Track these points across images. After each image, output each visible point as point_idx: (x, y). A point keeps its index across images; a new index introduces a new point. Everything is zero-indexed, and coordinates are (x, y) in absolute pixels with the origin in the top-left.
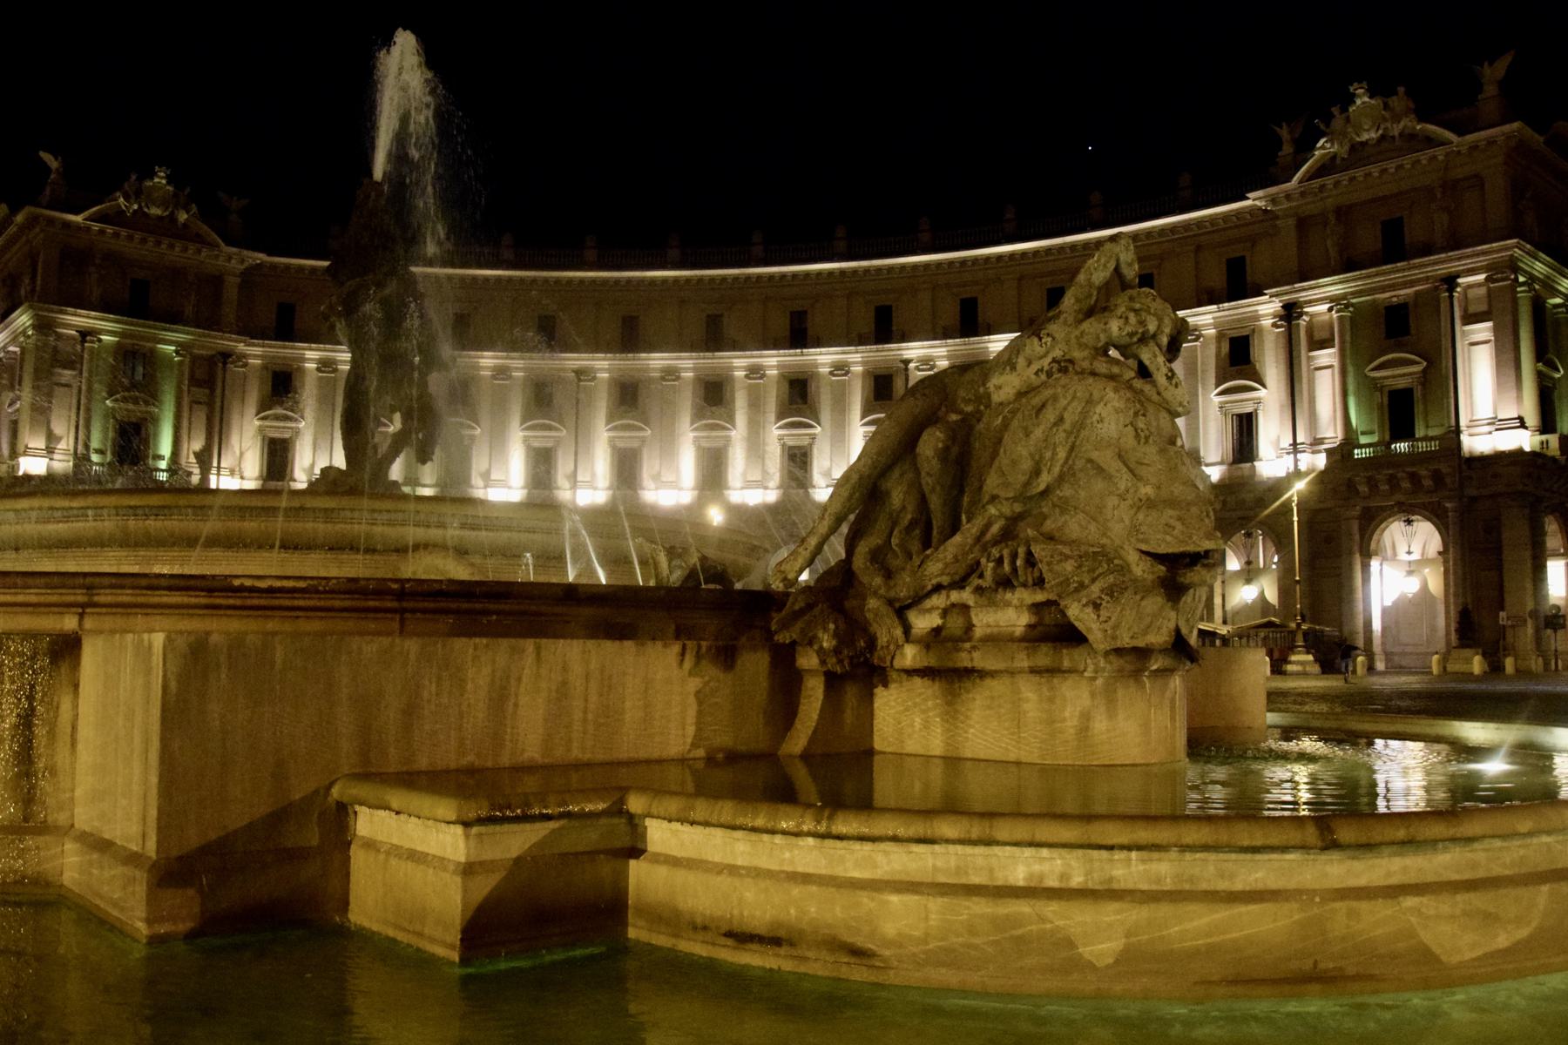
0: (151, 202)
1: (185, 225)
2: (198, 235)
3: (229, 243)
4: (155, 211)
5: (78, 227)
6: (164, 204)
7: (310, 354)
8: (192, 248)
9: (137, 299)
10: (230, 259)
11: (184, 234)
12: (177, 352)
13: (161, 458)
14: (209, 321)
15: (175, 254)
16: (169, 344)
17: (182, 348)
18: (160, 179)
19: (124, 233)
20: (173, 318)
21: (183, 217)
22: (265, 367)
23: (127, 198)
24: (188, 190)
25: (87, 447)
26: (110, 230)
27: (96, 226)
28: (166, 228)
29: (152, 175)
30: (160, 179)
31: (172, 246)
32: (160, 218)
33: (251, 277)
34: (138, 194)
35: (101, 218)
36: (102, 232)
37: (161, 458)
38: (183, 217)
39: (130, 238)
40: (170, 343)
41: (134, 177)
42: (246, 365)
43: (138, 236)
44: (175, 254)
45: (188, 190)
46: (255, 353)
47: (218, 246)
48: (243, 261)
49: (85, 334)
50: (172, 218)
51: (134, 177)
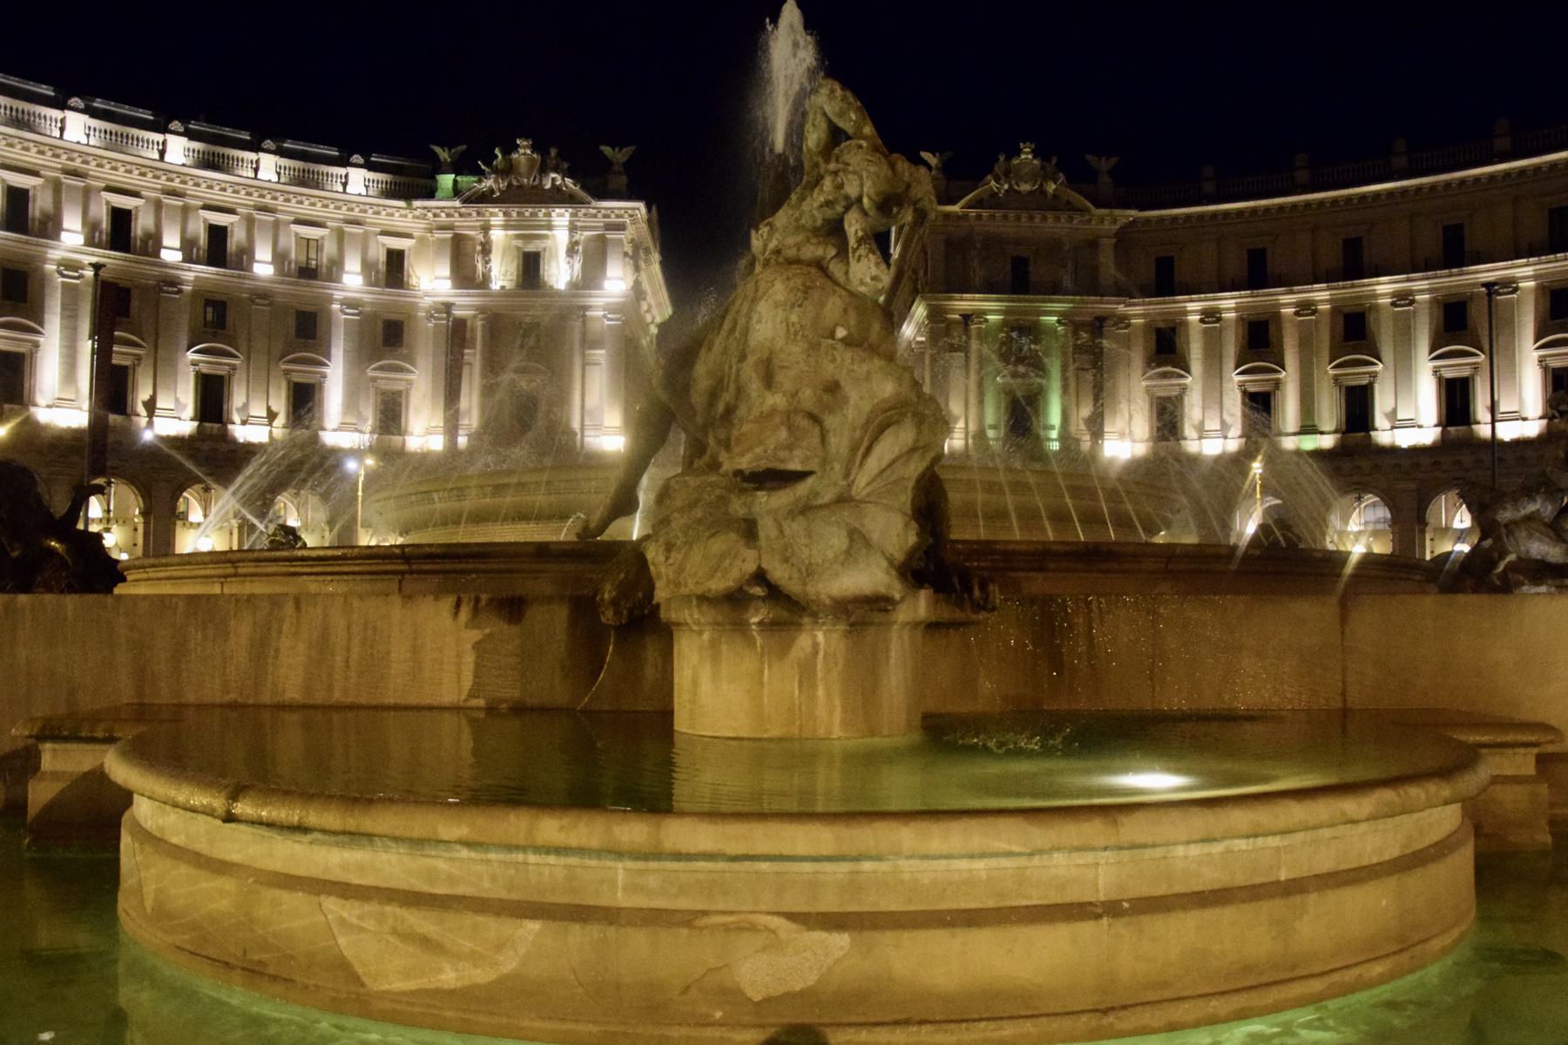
0: (1021, 179)
1: (1055, 196)
2: (1068, 202)
3: (1098, 205)
4: (1025, 187)
5: (959, 217)
6: (1032, 177)
7: (1191, 306)
8: (1064, 217)
9: (1018, 278)
10: (1102, 220)
11: (1055, 205)
12: (1059, 322)
13: (1052, 428)
14: (1090, 285)
15: (1053, 226)
16: (1051, 314)
17: (1065, 318)
18: (1026, 155)
19: (999, 214)
20: (1054, 289)
21: (1051, 187)
22: (1147, 326)
23: (997, 180)
24: (1054, 160)
25: (981, 418)
26: (985, 213)
27: (973, 212)
28: (1040, 202)
29: (1018, 152)
30: (1026, 155)
31: (1044, 219)
32: (1031, 192)
33: (1124, 238)
34: (1007, 174)
35: (978, 204)
36: (979, 217)
37: (1052, 428)
38: (1051, 187)
39: (1005, 217)
40: (1050, 313)
41: (1002, 158)
42: (1128, 326)
43: (1011, 215)
44: (1053, 226)
45: (1054, 160)
46: (1138, 312)
47: (1088, 210)
48: (1115, 221)
49: (967, 318)
50: (1042, 191)
51: (1002, 158)
